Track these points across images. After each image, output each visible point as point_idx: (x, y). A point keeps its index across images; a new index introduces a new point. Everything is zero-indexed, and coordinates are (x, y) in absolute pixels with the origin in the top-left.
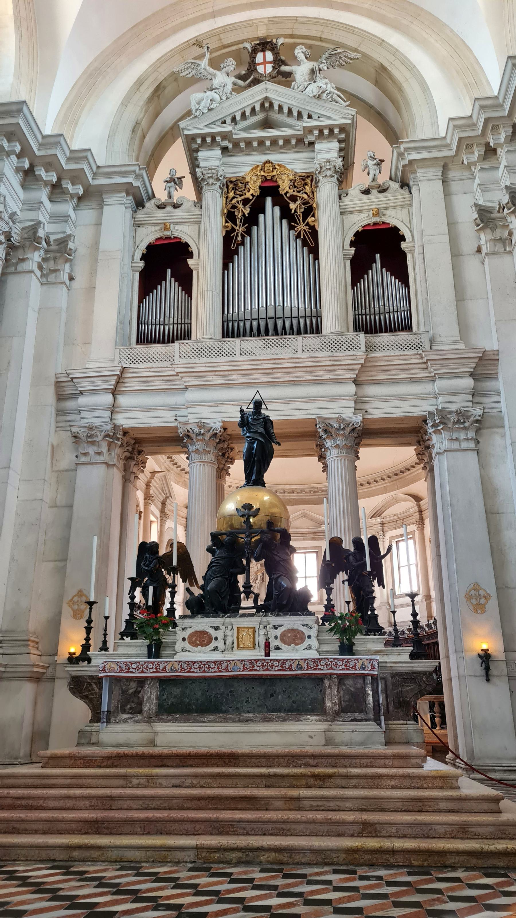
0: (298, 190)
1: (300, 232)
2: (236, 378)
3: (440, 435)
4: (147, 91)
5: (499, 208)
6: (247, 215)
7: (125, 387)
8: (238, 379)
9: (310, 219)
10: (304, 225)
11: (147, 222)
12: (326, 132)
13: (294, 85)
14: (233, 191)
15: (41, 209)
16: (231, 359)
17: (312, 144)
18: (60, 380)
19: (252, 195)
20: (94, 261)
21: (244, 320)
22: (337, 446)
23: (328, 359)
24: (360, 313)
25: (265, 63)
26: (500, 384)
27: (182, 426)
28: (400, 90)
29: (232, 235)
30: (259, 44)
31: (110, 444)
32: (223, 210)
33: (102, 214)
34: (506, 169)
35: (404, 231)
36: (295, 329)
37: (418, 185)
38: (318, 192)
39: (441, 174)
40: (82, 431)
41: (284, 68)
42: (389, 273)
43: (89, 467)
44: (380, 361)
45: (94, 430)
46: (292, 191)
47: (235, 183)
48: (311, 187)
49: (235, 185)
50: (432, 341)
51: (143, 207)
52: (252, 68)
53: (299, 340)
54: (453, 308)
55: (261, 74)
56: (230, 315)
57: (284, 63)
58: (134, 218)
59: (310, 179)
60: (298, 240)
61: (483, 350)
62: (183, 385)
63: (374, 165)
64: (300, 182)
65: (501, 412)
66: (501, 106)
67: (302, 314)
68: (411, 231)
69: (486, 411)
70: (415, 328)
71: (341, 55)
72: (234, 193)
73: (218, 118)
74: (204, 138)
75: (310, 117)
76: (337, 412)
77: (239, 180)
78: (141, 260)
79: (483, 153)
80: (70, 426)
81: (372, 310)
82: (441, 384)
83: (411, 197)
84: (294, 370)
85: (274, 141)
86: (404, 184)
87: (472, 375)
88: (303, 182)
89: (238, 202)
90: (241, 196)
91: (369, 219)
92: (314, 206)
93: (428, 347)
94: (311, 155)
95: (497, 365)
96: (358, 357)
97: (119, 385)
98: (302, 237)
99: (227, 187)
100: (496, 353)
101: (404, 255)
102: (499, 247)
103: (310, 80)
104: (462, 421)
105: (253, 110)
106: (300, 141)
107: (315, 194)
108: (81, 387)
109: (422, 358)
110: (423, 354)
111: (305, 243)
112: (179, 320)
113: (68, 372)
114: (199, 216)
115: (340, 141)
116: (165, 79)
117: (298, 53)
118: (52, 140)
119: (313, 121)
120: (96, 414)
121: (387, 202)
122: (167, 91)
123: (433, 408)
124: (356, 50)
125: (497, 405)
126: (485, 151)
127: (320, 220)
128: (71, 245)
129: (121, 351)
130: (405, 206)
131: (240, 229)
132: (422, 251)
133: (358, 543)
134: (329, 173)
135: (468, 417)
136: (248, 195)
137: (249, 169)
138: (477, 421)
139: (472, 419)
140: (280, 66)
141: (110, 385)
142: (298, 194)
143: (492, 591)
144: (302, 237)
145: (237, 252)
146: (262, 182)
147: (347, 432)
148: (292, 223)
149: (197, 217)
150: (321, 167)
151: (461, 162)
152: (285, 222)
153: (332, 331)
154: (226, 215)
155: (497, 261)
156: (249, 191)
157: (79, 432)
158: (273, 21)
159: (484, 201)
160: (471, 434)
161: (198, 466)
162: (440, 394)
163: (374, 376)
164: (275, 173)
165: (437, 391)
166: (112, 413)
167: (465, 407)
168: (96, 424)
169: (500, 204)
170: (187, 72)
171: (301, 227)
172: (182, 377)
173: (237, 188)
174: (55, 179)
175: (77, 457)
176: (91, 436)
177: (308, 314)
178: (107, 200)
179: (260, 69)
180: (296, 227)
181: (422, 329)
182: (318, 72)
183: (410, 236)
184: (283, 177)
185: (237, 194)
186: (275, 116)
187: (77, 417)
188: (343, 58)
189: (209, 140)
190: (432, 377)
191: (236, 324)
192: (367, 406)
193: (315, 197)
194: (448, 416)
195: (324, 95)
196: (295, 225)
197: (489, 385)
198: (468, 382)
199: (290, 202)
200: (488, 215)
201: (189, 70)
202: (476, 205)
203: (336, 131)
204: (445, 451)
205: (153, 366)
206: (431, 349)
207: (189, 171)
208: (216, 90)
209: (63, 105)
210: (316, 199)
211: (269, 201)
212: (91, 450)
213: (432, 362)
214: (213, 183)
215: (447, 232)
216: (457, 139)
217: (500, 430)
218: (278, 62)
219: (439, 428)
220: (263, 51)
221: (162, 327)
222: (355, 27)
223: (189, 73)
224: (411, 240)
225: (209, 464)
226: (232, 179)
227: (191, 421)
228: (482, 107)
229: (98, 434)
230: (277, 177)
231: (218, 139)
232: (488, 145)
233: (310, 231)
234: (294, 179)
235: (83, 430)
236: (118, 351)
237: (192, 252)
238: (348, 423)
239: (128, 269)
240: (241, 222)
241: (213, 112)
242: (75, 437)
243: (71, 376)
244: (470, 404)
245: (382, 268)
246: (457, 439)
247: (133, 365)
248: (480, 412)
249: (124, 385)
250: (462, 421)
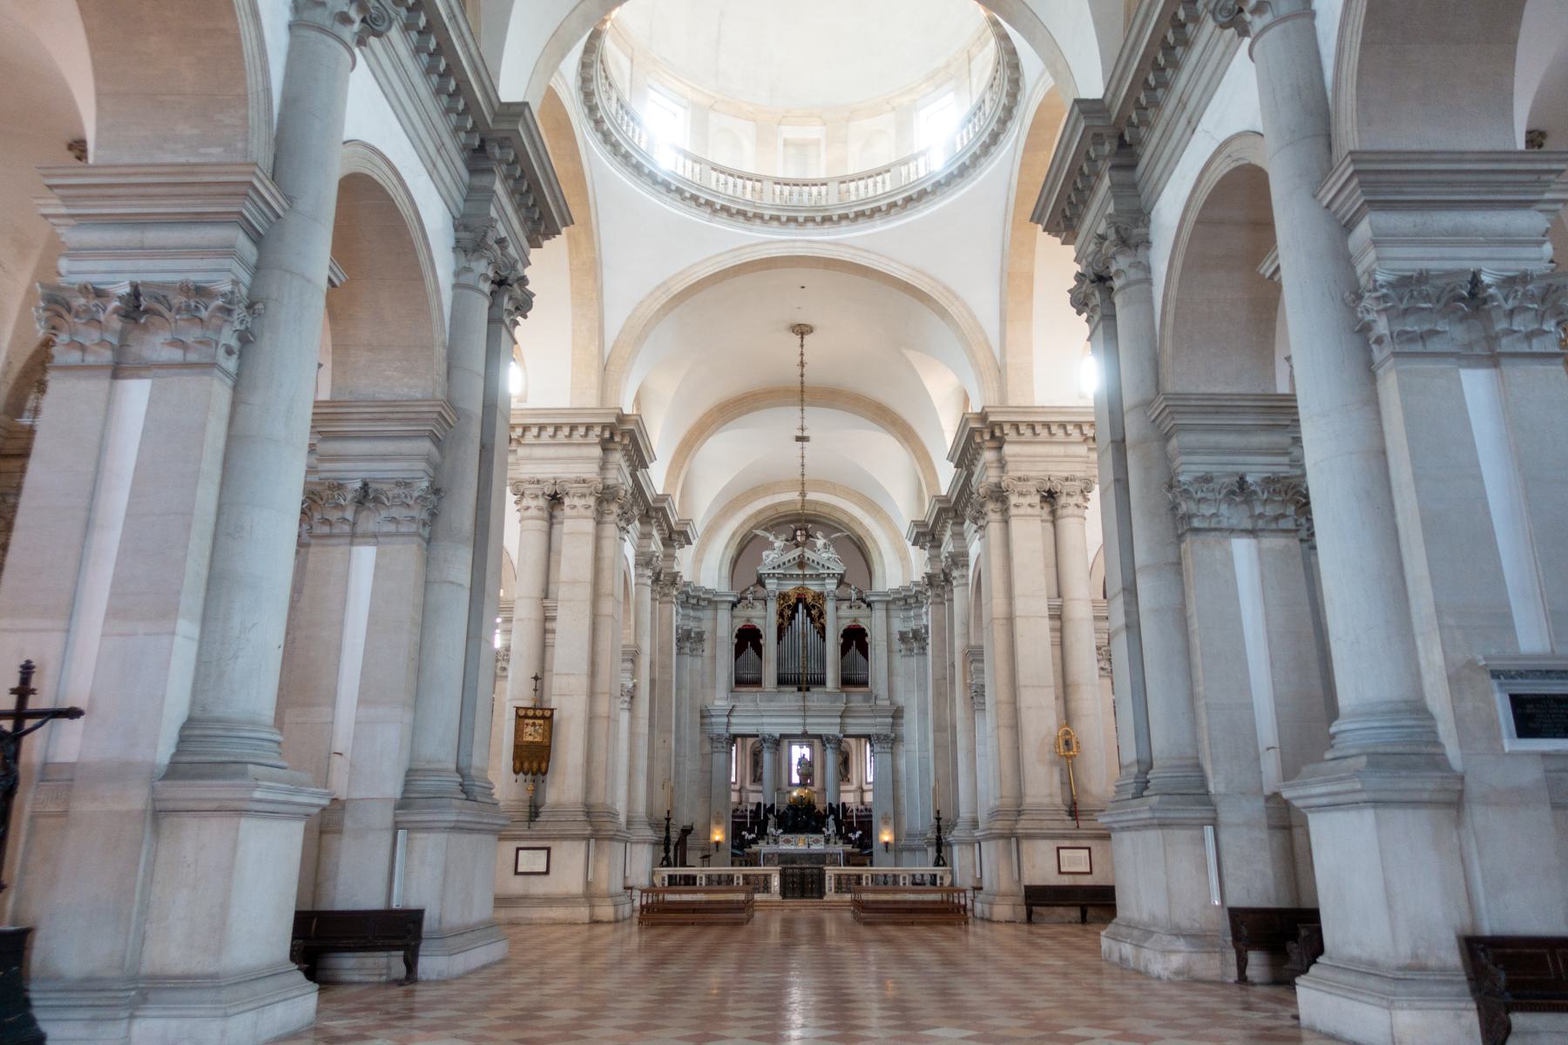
4: (738, 539)
9: (822, 620)
20: (715, 641)
26: (904, 721)
35: (868, 631)
74: (769, 574)
82: (878, 720)
101: (867, 644)
102: (909, 653)
106: (818, 575)
131: (786, 624)
133: (838, 806)
137: (791, 587)
143: (892, 816)
155: (907, 659)
179: (799, 538)
197: (900, 721)
211: (800, 606)
212: (719, 745)
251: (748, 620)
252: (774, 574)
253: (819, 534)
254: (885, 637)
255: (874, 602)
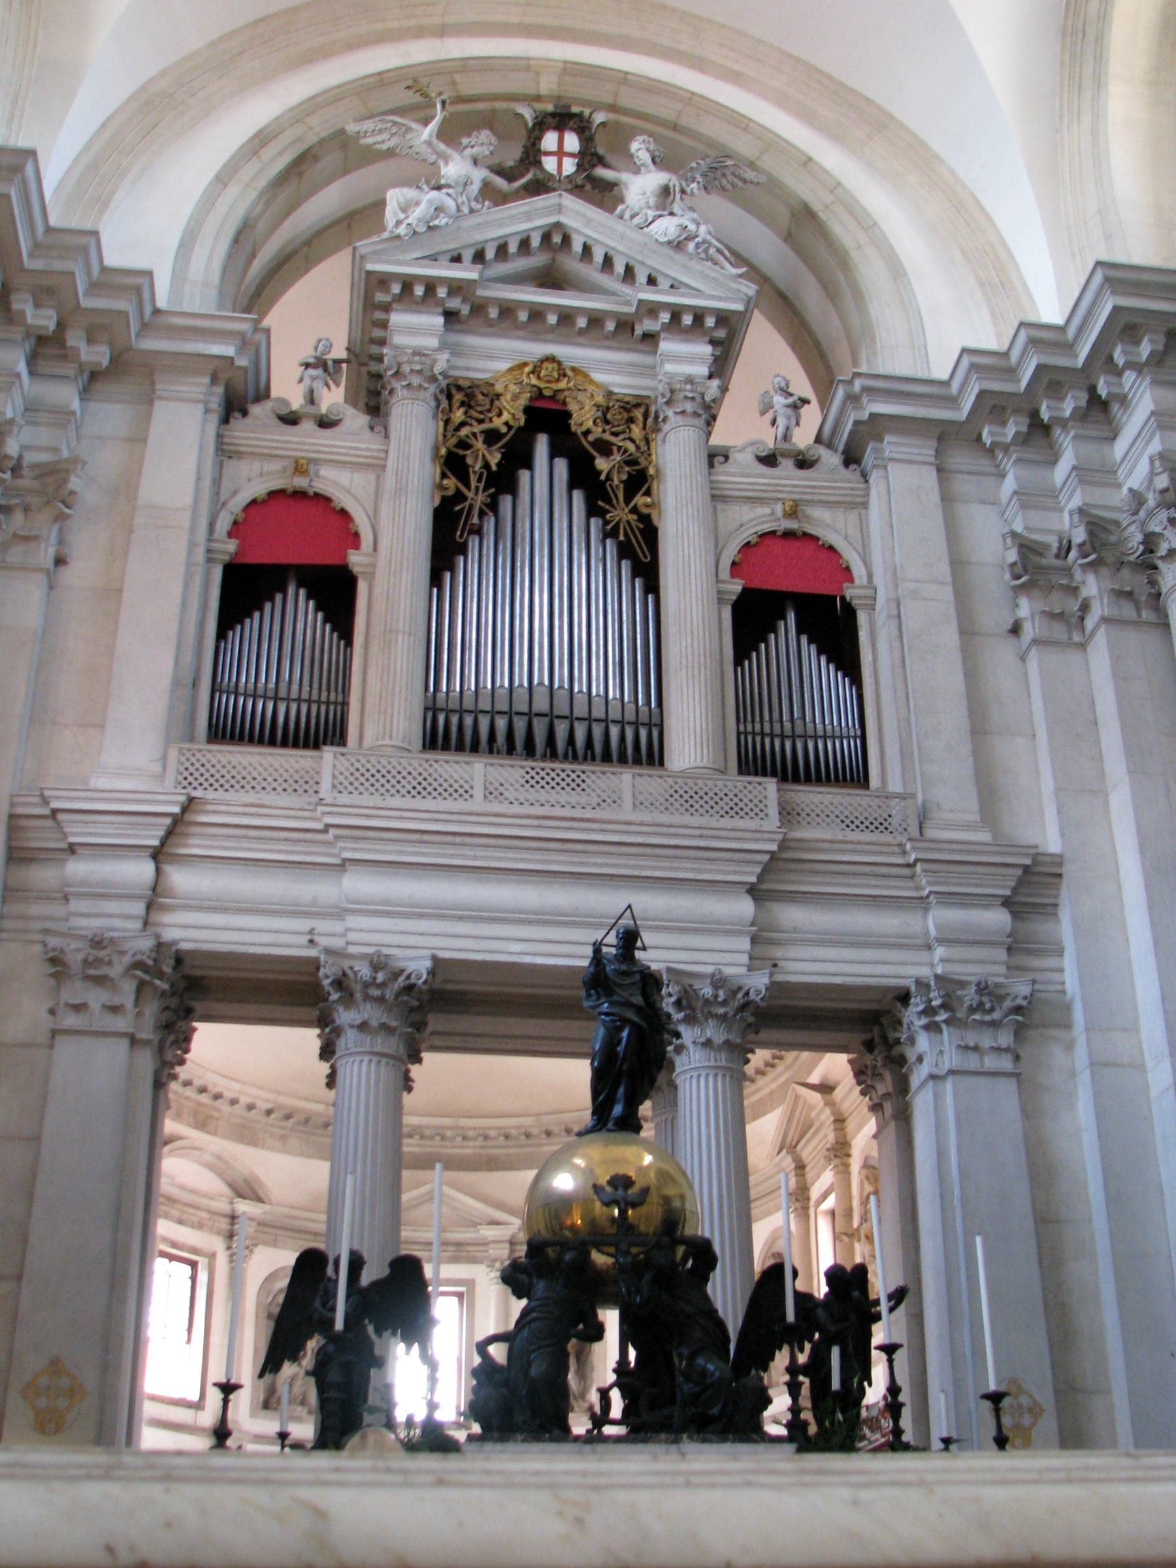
0: (613, 430)
1: (617, 524)
2: (471, 853)
3: (938, 1036)
5: (1060, 548)
6: (494, 468)
7: (186, 846)
8: (475, 858)
9: (640, 500)
10: (626, 510)
11: (251, 449)
12: (687, 320)
13: (623, 211)
14: (462, 410)
15: (14, 390)
16: (460, 805)
17: (650, 338)
18: (20, 810)
19: (506, 424)
21: (476, 713)
22: (708, 1044)
23: (697, 832)
24: (749, 728)
25: (560, 153)
26: (1065, 928)
27: (331, 960)
28: (844, 261)
29: (457, 508)
30: (553, 115)
31: (141, 987)
32: (436, 449)
33: (149, 415)
34: (1074, 474)
36: (598, 748)
37: (885, 467)
38: (659, 443)
39: (933, 452)
40: (76, 950)
41: (601, 172)
42: (813, 648)
43: (88, 1041)
44: (811, 850)
45: (105, 948)
46: (600, 430)
47: (469, 391)
48: (644, 428)
49: (467, 395)
50: (923, 820)
51: (245, 413)
52: (532, 159)
53: (625, 779)
54: (965, 749)
55: (551, 175)
56: (441, 696)
57: (601, 161)
58: (219, 436)
59: (642, 410)
60: (608, 541)
61: (1033, 851)
62: (338, 855)
63: (788, 406)
64: (620, 413)
65: (1063, 992)
66: (1069, 347)
67: (615, 714)
68: (865, 563)
69: (1037, 987)
70: (874, 780)
71: (725, 171)
72: (466, 413)
73: (445, 248)
74: (407, 284)
75: (652, 281)
76: (709, 960)
77: (478, 386)
78: (230, 535)
79: (1024, 429)
80: (46, 931)
81: (777, 727)
83: (868, 489)
84: (613, 849)
85: (566, 317)
86: (851, 458)
87: (1007, 903)
88: (625, 415)
89: (474, 435)
90: (480, 421)
91: (775, 521)
92: (651, 471)
93: (914, 832)
94: (647, 359)
95: (1057, 887)
96: (766, 836)
97: (172, 840)
98: (622, 538)
99: (450, 397)
100: (1057, 860)
102: (1058, 631)
103: (657, 208)
104: (988, 1006)
105: (525, 244)
106: (625, 325)
107: (653, 445)
108: (75, 834)
109: (904, 853)
110: (908, 846)
111: (625, 551)
112: (306, 688)
113: (47, 793)
114: (382, 455)
115: (713, 342)
116: (322, 142)
117: (638, 150)
118: (68, 240)
119: (656, 292)
120: (112, 906)
121: (816, 491)
122: (320, 166)
123: (924, 972)
124: (752, 165)
125: (1056, 977)
126: (1030, 426)
127: (663, 503)
128: (74, 483)
129: (183, 755)
130: (852, 505)
131: (477, 497)
132: (895, 612)
134: (689, 407)
135: (1001, 998)
136: (498, 423)
137: (503, 366)
138: (1018, 1010)
139: (1008, 1004)
140: (594, 166)
141: (152, 837)
142: (613, 439)
144: (622, 538)
145: (463, 550)
146: (531, 399)
147: (729, 1010)
148: (600, 503)
149: (375, 454)
150: (672, 392)
151: (975, 436)
152: (578, 496)
153: (692, 764)
154: (442, 460)
156: (500, 415)
157: (66, 949)
158: (571, 69)
159: (1026, 528)
160: (1005, 1038)
161: (365, 1064)
162: (941, 941)
163: (800, 883)
164: (563, 384)
165: (933, 932)
166: (149, 907)
167: (993, 975)
168: (112, 934)
169: (1060, 541)
170: (379, 138)
171: (620, 514)
172: (337, 837)
173: (472, 403)
174: (52, 326)
175: (52, 1012)
176: (98, 962)
177: (630, 715)
178: (164, 387)
179: (550, 164)
180: (609, 512)
181: (895, 786)
182: (678, 196)
183: (863, 572)
184: (581, 396)
185: (471, 417)
186: (571, 264)
187: (59, 910)
188: (730, 178)
189: (419, 291)
190: (921, 898)
191: (455, 720)
192: (778, 952)
193: (653, 452)
194: (959, 993)
195: (691, 246)
196: (607, 507)
197: (1039, 927)
198: (998, 918)
199: (595, 454)
200: (1037, 559)
201: (385, 136)
202: (1014, 535)
203: (710, 322)
204: (952, 1072)
205: (266, 802)
206: (921, 834)
207: (346, 345)
208: (450, 191)
209: (76, 160)
210: (654, 457)
212: (96, 998)
213: (927, 866)
214: (420, 386)
215: (949, 579)
216: (976, 391)
217: (1061, 1034)
218: (589, 158)
219: (938, 1018)
220: (560, 129)
221: (270, 705)
222: (750, 120)
223: (383, 142)
224: (865, 581)
225: (392, 1062)
226: (461, 382)
227: (352, 950)
228: (1033, 342)
229: (115, 958)
230: (566, 393)
231: (442, 292)
232: (1035, 414)
233: (641, 526)
234: (604, 404)
235: (74, 945)
236: (173, 754)
237: (357, 535)
238: (735, 988)
239: (200, 555)
240: (479, 480)
241: (436, 233)
242: (53, 961)
243: (55, 805)
244: (1002, 969)
245: (799, 632)
246: (976, 1048)
247: (210, 795)
248: (1025, 990)
249: (182, 841)
250: (988, 1006)
251: (299, 468)
252: (431, 286)
253: (639, 148)
254: (943, 569)
255: (876, 426)
